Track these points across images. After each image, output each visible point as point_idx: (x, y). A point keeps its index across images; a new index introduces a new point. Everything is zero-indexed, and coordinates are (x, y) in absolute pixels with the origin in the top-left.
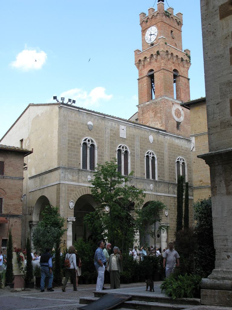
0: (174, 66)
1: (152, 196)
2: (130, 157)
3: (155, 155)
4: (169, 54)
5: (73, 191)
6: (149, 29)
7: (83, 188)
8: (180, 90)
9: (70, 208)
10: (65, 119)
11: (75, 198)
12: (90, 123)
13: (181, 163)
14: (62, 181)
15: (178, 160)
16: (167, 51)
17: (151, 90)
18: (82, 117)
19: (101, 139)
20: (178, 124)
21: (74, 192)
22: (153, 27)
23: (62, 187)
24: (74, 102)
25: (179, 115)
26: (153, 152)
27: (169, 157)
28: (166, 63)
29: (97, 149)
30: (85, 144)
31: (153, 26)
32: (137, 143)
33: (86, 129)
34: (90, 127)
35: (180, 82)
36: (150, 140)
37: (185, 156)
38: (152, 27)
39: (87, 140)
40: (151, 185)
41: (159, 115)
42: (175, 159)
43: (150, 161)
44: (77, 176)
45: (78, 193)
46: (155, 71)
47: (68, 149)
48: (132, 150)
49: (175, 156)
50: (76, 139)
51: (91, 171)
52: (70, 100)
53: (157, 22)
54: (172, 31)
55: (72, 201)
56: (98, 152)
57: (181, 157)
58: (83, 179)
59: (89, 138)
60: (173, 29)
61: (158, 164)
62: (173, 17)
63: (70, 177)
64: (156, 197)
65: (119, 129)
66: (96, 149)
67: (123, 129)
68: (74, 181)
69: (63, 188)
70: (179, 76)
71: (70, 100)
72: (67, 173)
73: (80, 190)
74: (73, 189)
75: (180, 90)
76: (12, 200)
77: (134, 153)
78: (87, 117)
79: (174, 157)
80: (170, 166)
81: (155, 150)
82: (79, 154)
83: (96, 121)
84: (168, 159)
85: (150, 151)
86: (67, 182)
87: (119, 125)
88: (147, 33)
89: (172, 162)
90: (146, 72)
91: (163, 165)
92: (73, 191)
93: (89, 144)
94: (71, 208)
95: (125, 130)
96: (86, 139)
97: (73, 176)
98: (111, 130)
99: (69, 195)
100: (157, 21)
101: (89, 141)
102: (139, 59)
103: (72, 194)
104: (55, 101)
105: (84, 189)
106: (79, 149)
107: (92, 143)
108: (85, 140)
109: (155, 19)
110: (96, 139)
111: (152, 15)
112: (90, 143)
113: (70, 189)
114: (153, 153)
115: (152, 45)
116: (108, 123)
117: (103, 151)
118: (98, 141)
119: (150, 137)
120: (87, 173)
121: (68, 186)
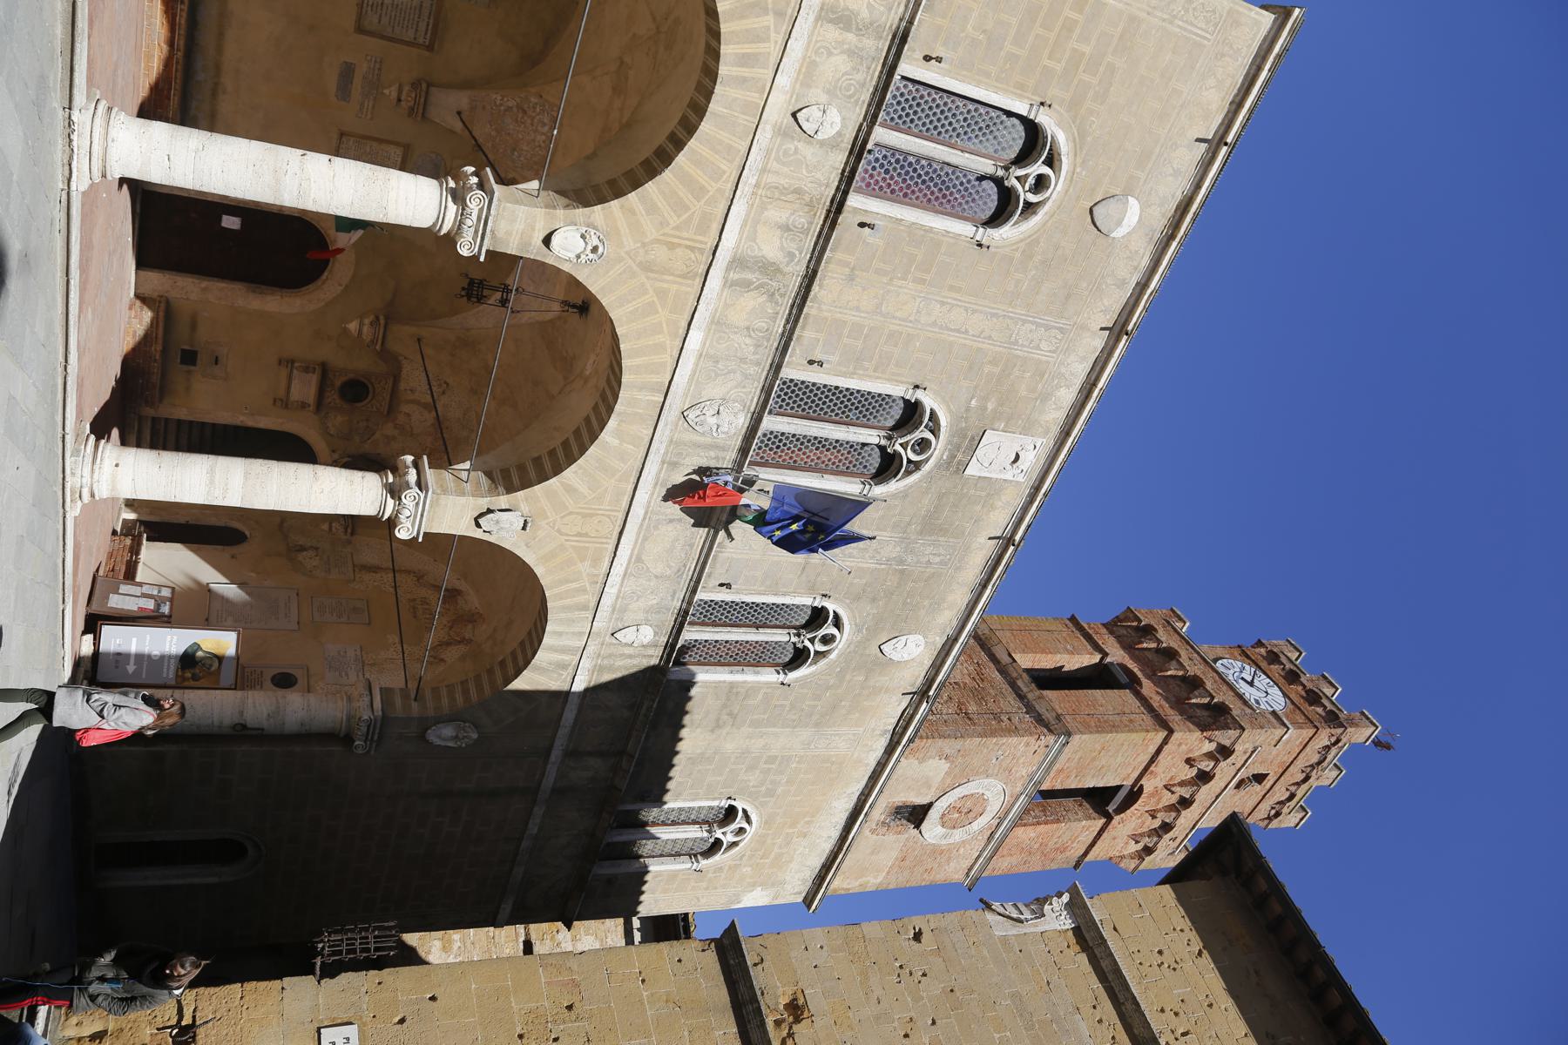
0: (1156, 792)
3: (813, 668)
13: (718, 834)
15: (740, 814)
37: (751, 857)
44: (865, 14)
50: (1086, 78)
54: (1259, 778)
58: (833, 59)
61: (754, 689)
64: (564, 666)
65: (1026, 431)
90: (1116, 655)
110: (1031, 242)
112: (1025, 195)
117: (952, 288)
118: (1018, 255)
119: (919, 638)
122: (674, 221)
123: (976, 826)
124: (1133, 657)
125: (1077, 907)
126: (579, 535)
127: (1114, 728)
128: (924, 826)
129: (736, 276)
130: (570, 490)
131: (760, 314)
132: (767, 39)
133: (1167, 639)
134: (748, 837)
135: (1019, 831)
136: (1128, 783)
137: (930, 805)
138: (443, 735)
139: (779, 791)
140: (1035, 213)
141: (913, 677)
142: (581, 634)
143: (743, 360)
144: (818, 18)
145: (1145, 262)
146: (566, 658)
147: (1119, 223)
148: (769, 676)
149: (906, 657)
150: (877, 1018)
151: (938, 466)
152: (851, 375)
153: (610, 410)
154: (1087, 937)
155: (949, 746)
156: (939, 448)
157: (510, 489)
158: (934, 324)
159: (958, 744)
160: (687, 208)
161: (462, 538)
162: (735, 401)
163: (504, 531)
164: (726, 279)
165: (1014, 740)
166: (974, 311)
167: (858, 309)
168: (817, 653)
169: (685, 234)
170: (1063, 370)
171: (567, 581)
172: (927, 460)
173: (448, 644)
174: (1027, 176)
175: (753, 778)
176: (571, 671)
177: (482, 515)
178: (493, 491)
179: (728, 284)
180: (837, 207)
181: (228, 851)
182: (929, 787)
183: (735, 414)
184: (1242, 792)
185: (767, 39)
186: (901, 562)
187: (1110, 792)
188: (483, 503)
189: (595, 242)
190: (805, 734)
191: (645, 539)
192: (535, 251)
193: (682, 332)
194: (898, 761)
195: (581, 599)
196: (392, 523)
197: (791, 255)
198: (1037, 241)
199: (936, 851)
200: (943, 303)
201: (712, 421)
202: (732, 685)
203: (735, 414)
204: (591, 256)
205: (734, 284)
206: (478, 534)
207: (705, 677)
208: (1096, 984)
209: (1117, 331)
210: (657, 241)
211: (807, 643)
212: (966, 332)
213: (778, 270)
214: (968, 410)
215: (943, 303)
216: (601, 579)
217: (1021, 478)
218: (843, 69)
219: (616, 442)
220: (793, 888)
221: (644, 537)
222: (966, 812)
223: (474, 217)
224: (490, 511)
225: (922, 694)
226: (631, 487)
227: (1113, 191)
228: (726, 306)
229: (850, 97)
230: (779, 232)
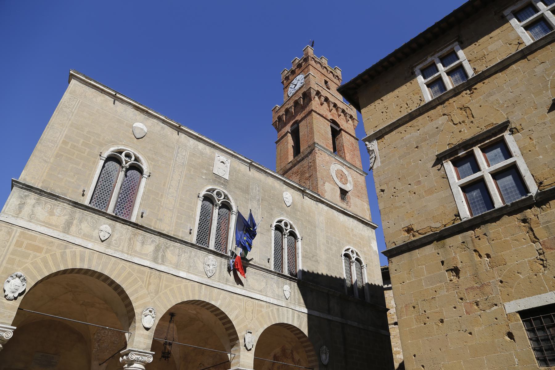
0: (332, 115)
3: (296, 229)
5: (38, 249)
13: (354, 259)
15: (346, 252)
21: (38, 254)
58: (83, 228)
64: (299, 316)
65: (213, 159)
68: (50, 225)
74: (41, 245)
92: (38, 249)
94: (11, 296)
97: (51, 213)
103: (31, 256)
105: (78, 254)
110: (148, 159)
112: (132, 161)
113: (30, 242)
117: (164, 185)
118: (153, 163)
119: (284, 194)
122: (140, 283)
123: (346, 173)
124: (289, 122)
125: (370, 139)
126: (252, 313)
127: (312, 128)
128: (347, 190)
129: (160, 260)
130: (237, 317)
131: (173, 251)
132: (75, 252)
133: (282, 112)
134: (354, 249)
135: (347, 158)
136: (329, 124)
137: (340, 188)
138: (325, 358)
139: (338, 239)
140: (138, 158)
141: (298, 195)
142: (287, 311)
143: (190, 257)
144: (68, 234)
145: (155, 121)
146: (296, 315)
147: (142, 129)
148: (299, 244)
149: (291, 198)
150: (410, 203)
151: (226, 189)
152: (195, 219)
153: (208, 304)
154: (379, 136)
155: (320, 183)
156: (219, 188)
157: (237, 338)
158: (177, 191)
159: (319, 179)
160: (136, 279)
161: (255, 355)
162: (204, 259)
163: (252, 340)
164: (161, 264)
165: (317, 161)
166: (172, 177)
167: (171, 217)
168: (290, 228)
169: (145, 279)
170: (192, 147)
171: (269, 316)
172: (224, 192)
173: (293, 358)
174: (125, 160)
175: (334, 248)
176: (300, 314)
177: (247, 349)
178: (238, 345)
179: (163, 263)
180: (136, 226)
182: (334, 188)
183: (209, 259)
184: (331, 87)
185: (75, 252)
186: (259, 200)
187: (333, 130)
188: (242, 348)
189: (148, 311)
192: (151, 333)
193: (180, 279)
194: (326, 199)
195: (275, 311)
197: (153, 241)
199: (355, 186)
200: (169, 188)
201: (211, 267)
202: (303, 257)
203: (209, 259)
204: (153, 313)
205: (163, 261)
207: (300, 266)
208: (394, 132)
209: (179, 130)
210: (147, 289)
211: (287, 231)
212: (179, 180)
213: (158, 245)
214: (206, 179)
215: (169, 188)
216: (268, 304)
217: (229, 161)
218: (86, 224)
219: (219, 301)
220: (370, 233)
221: (252, 289)
222: (342, 176)
223: (138, 357)
224: (245, 346)
225: (303, 192)
226: (235, 295)
228: (171, 263)
229: (96, 222)
230: (144, 246)
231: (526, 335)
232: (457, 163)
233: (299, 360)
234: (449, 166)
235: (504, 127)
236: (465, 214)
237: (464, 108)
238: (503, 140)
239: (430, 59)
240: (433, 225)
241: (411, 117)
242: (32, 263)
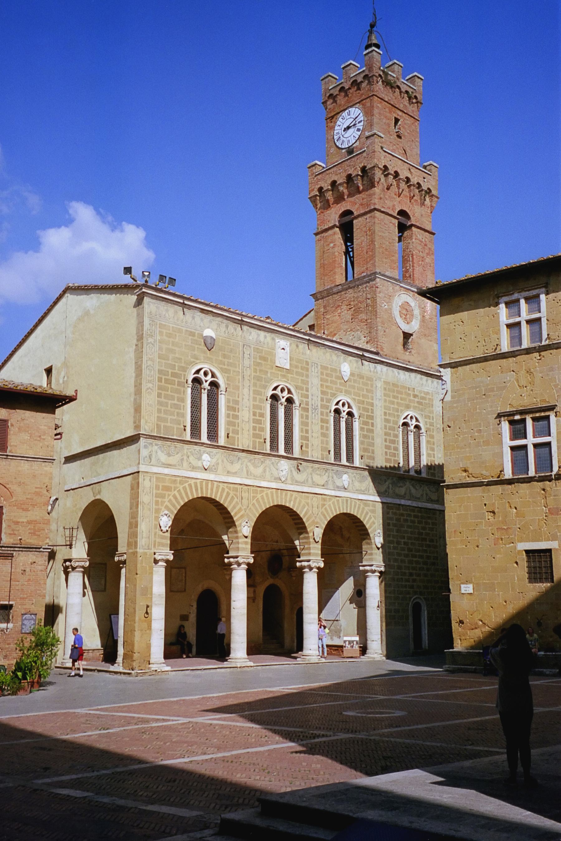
1: (347, 501)
2: (297, 411)
3: (353, 407)
4: (389, 174)
5: (168, 489)
6: (344, 114)
7: (192, 482)
8: (413, 258)
9: (162, 530)
10: (153, 321)
11: (174, 506)
12: (208, 333)
14: (144, 466)
15: (405, 420)
16: (385, 167)
17: (344, 259)
18: (191, 319)
19: (234, 371)
20: (407, 336)
21: (170, 493)
22: (354, 109)
23: (144, 480)
24: (172, 281)
25: (408, 316)
26: (349, 401)
27: (385, 414)
28: (382, 196)
29: (224, 393)
30: (197, 381)
31: (351, 107)
32: (315, 382)
33: (200, 347)
34: (209, 341)
35: (414, 240)
36: (343, 373)
38: (350, 109)
39: (202, 372)
40: (345, 477)
41: (363, 316)
42: (398, 416)
43: (342, 418)
45: (180, 494)
46: (356, 213)
47: (158, 393)
48: (302, 397)
49: (398, 412)
51: (209, 443)
52: (162, 278)
53: (364, 97)
54: (397, 120)
55: (166, 512)
56: (228, 401)
57: (411, 413)
58: (191, 461)
59: (206, 367)
60: (400, 113)
62: (401, 87)
63: (163, 458)
66: (222, 392)
67: (283, 349)
68: (171, 465)
69: (145, 483)
70: (412, 225)
71: (162, 278)
72: (156, 447)
73: (184, 488)
75: (411, 259)
76: (27, 510)
77: (307, 404)
78: (202, 320)
79: (396, 413)
80: (386, 434)
81: (354, 397)
82: (182, 404)
83: (223, 328)
84: (383, 417)
85: (344, 398)
86: (155, 470)
87: (273, 339)
88: (338, 123)
89: (391, 425)
90: (333, 216)
91: (372, 431)
92: (168, 489)
93: (206, 381)
94: (164, 529)
95: (288, 349)
96: (200, 369)
98: (257, 350)
99: (160, 500)
100: (362, 94)
101: (206, 374)
102: (319, 186)
104: (127, 280)
106: (184, 392)
107: (213, 379)
108: (198, 372)
109: (359, 89)
110: (222, 370)
111: (351, 81)
112: (209, 378)
114: (348, 404)
115: (350, 151)
116: (251, 333)
117: (238, 397)
118: (226, 375)
120: (202, 448)
121: (156, 478)
122: (236, 499)
137: (403, 332)
145: (219, 319)
147: (212, 337)
154: (453, 365)
158: (249, 400)
167: (249, 430)
168: (349, 408)
172: (287, 387)
173: (342, 535)
177: (315, 541)
181: (417, 608)
188: (312, 540)
189: (245, 523)
190: (376, 402)
191: (318, 485)
192: (249, 540)
195: (336, 502)
196: (319, 568)
198: (221, 368)
201: (284, 472)
206: (320, 541)
217: (288, 344)
224: (314, 539)
226: (304, 494)
227: (203, 343)
231: (526, 564)
232: (511, 423)
233: (349, 538)
234: (505, 426)
235: (552, 408)
236: (508, 474)
237: (529, 372)
238: (547, 418)
239: (516, 296)
240: (484, 472)
241: (485, 359)
242: (168, 501)
